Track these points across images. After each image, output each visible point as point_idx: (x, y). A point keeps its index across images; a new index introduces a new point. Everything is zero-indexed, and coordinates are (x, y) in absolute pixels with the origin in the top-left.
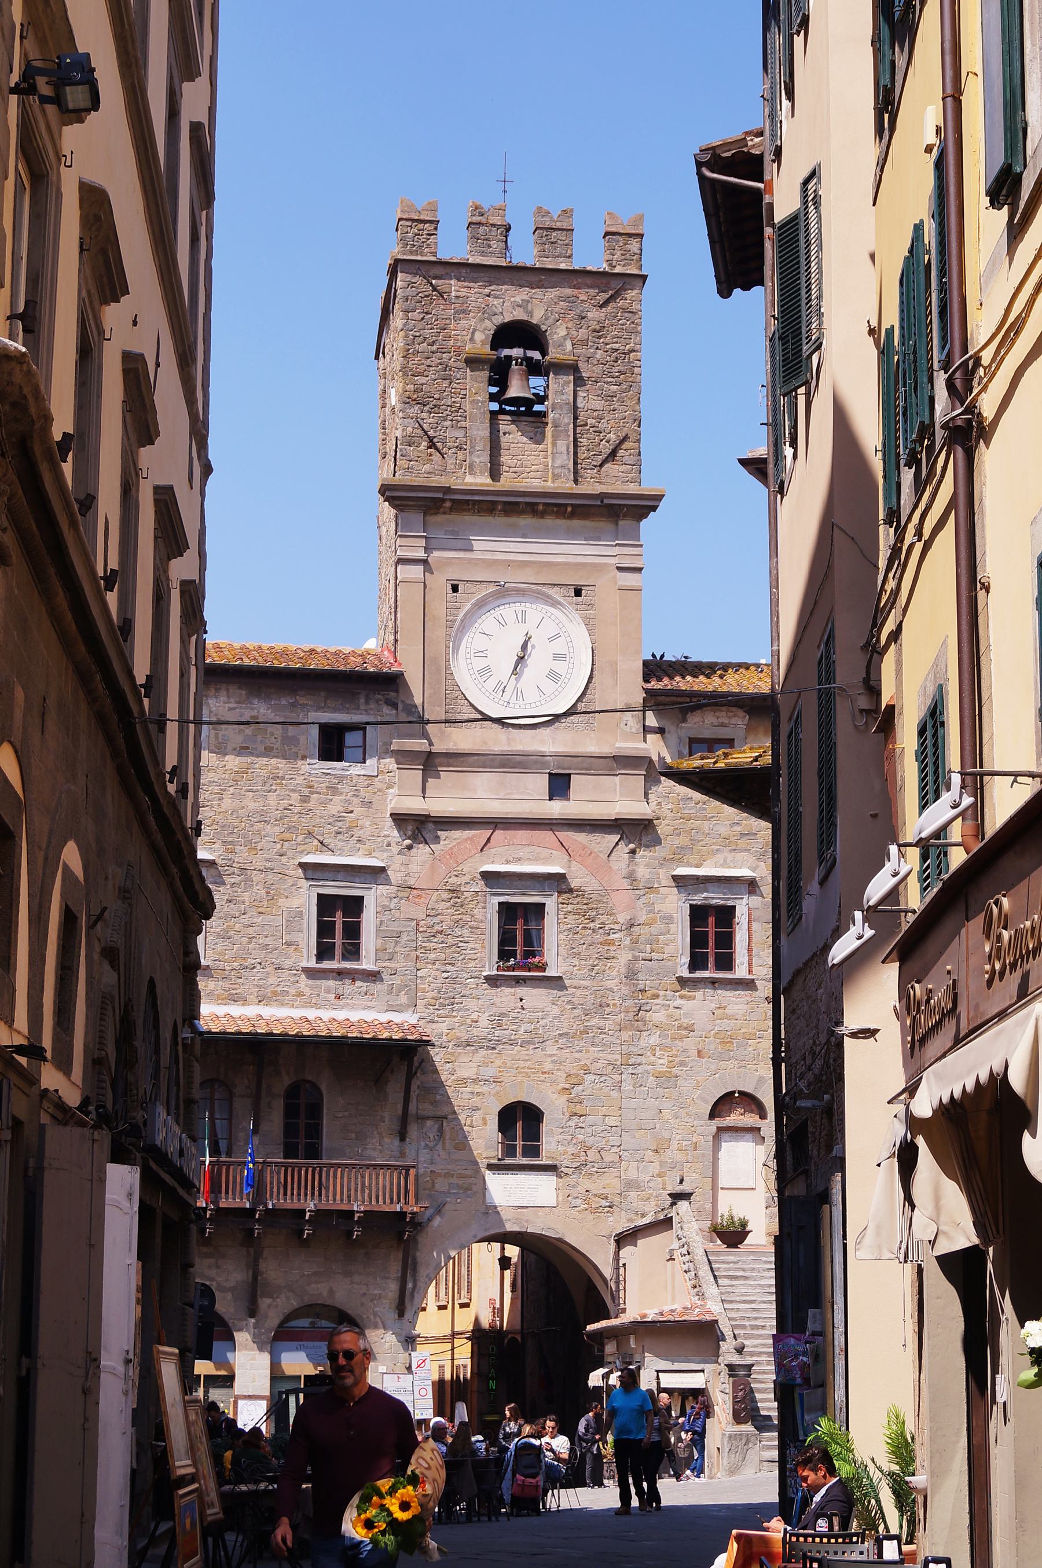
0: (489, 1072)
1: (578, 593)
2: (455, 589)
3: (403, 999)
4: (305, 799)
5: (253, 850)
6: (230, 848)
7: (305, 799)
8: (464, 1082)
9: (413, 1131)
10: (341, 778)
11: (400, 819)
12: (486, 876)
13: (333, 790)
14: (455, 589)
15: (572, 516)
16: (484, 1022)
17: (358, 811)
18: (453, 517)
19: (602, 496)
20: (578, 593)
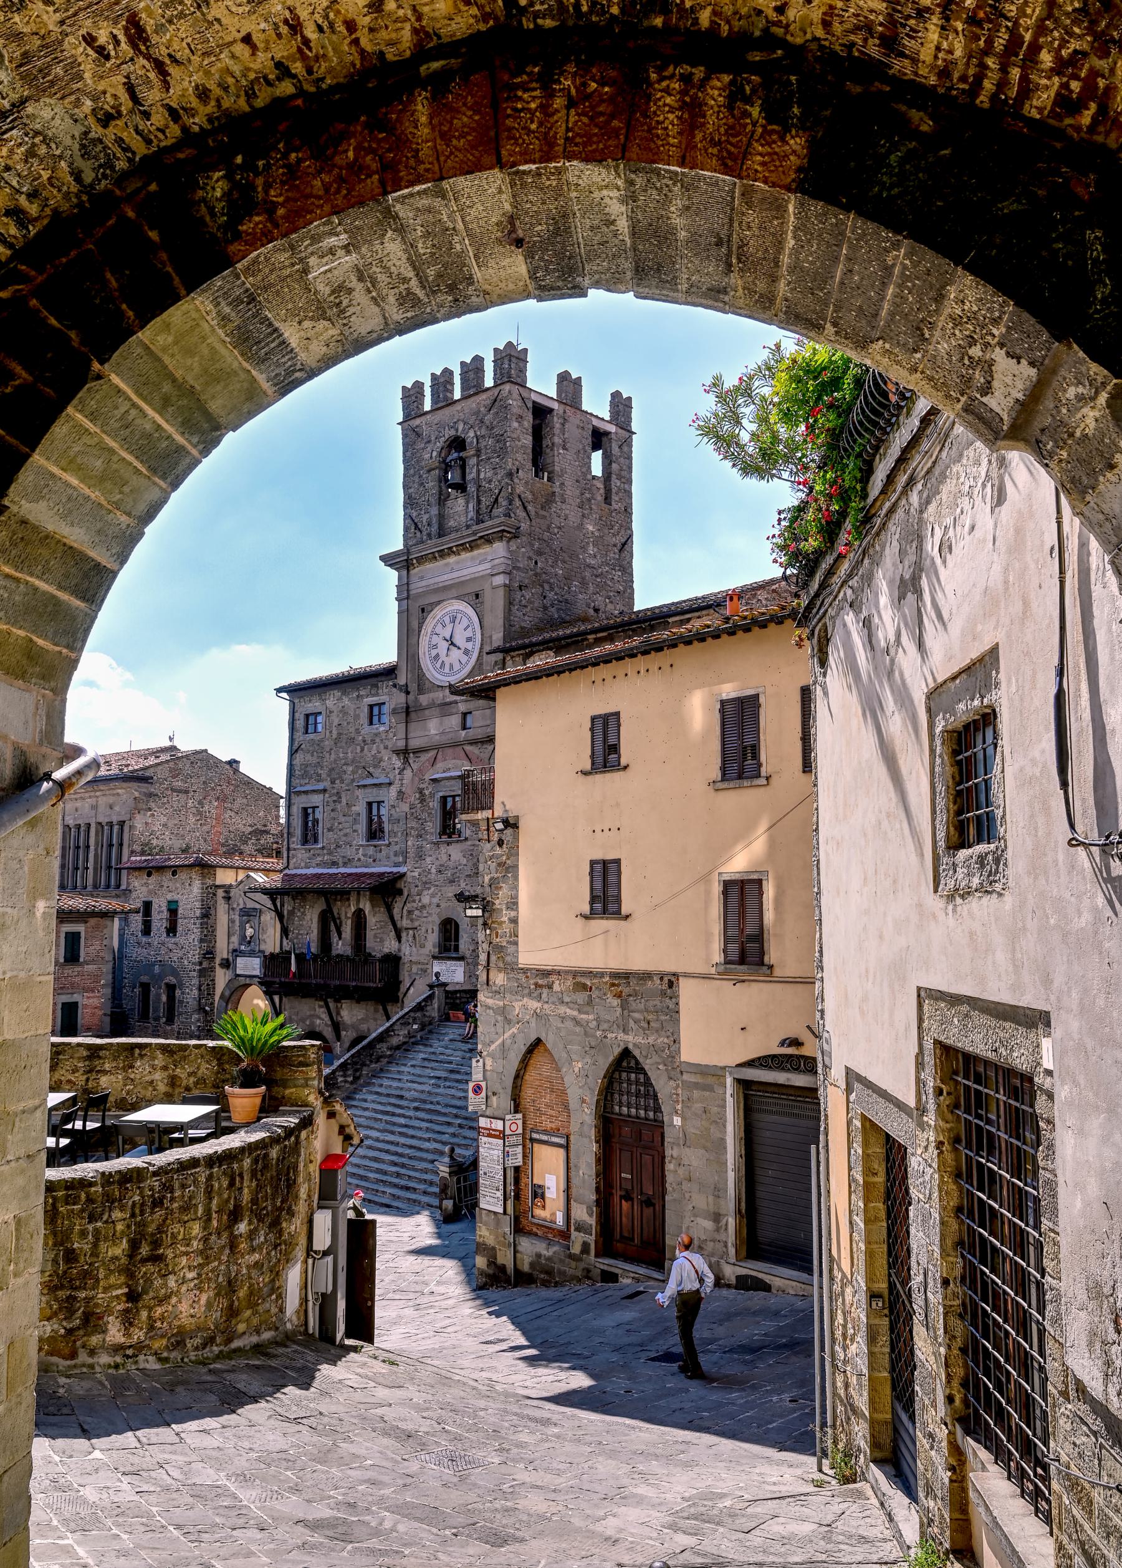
0: (435, 900)
1: (477, 596)
2: (423, 610)
3: (401, 859)
4: (362, 750)
5: (342, 781)
6: (333, 782)
7: (362, 750)
8: (424, 907)
9: (404, 934)
10: (376, 735)
11: (397, 752)
12: (434, 780)
13: (373, 742)
14: (423, 610)
15: (472, 549)
16: (433, 871)
17: (383, 751)
18: (421, 568)
19: (474, 534)
20: (477, 596)
